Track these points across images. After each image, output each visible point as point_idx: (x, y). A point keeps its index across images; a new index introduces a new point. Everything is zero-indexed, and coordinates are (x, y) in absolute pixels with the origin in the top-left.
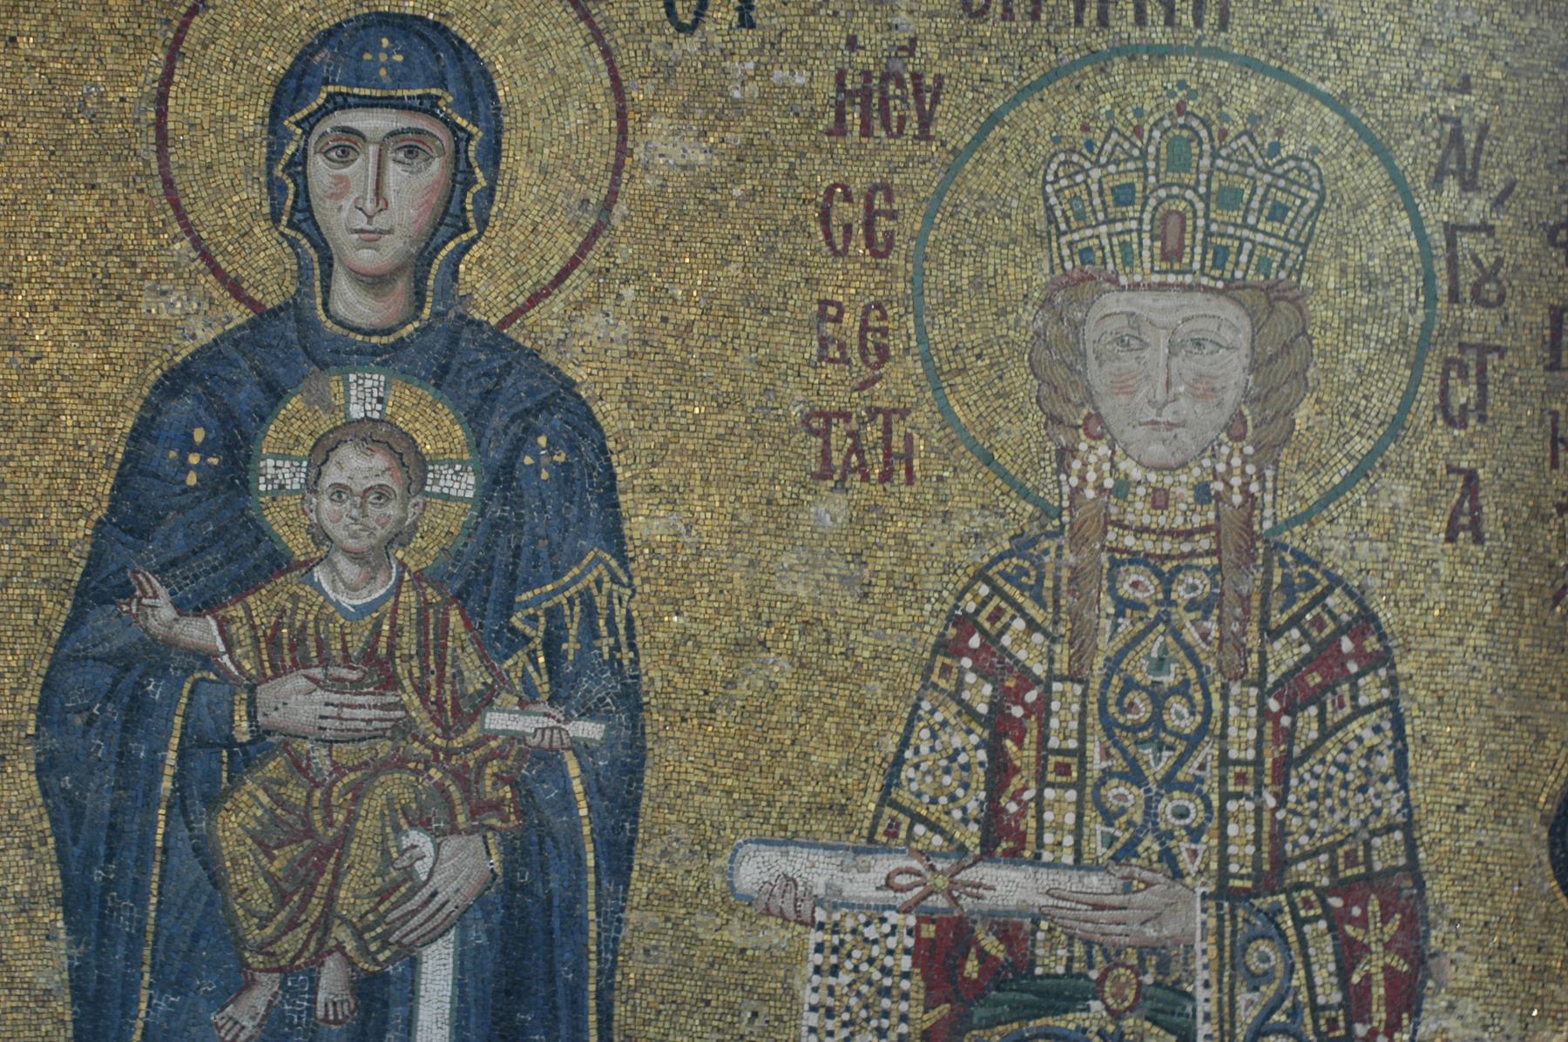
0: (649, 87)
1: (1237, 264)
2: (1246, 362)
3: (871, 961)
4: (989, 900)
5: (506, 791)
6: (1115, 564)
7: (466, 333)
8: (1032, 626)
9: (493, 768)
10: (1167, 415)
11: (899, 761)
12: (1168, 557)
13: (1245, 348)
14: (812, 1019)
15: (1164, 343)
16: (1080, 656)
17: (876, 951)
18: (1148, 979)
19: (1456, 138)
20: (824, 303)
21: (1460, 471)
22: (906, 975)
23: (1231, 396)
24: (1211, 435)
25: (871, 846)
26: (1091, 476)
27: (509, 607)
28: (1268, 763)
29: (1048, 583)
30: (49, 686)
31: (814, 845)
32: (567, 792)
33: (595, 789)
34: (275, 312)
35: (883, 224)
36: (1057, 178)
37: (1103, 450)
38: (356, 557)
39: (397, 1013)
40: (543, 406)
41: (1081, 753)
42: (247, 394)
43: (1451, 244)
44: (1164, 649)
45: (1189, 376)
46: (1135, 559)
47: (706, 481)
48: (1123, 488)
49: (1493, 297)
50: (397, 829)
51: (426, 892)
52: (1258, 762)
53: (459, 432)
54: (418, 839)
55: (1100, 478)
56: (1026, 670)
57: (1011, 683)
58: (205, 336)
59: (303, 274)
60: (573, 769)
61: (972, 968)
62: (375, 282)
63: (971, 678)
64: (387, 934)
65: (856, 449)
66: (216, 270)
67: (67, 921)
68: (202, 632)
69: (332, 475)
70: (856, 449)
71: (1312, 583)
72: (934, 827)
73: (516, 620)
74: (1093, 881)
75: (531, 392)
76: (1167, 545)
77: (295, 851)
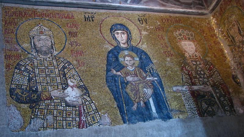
0: (141, 28)
3: (187, 95)
4: (195, 89)
5: (151, 84)
6: (192, 62)
7: (133, 47)
8: (188, 67)
9: (149, 82)
10: (190, 50)
11: (183, 78)
14: (185, 101)
17: (187, 94)
18: (210, 94)
19: (201, 30)
20: (161, 44)
22: (191, 96)
23: (194, 49)
24: (194, 51)
25: (183, 86)
27: (145, 69)
28: (210, 76)
30: (106, 79)
31: (179, 86)
32: (156, 84)
33: (159, 83)
34: (116, 46)
35: (163, 38)
38: (130, 66)
39: (149, 105)
40: (142, 52)
41: (196, 76)
42: (116, 53)
47: (158, 57)
48: (190, 56)
50: (143, 89)
51: (147, 94)
52: (209, 76)
53: (136, 55)
54: (145, 89)
58: (111, 49)
59: (117, 43)
60: (156, 82)
61: (196, 95)
62: (124, 44)
63: (185, 71)
64: (145, 98)
65: (168, 54)
66: (110, 43)
67: (115, 100)
68: (119, 73)
69: (126, 59)
70: (168, 54)
72: (188, 83)
73: (146, 70)
74: (202, 86)
75: (141, 51)
77: (135, 91)
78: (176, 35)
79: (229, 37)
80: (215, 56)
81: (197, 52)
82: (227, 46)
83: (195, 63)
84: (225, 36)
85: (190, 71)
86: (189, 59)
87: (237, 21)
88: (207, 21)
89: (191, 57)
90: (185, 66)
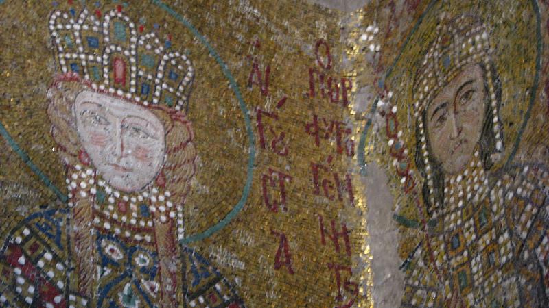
1: (155, 96)
2: (163, 147)
6: (99, 237)
8: (56, 259)
10: (123, 163)
12: (127, 239)
13: (162, 138)
15: (118, 125)
16: (82, 282)
19: (255, 66)
21: (278, 234)
23: (156, 163)
24: (147, 180)
26: (83, 185)
29: (64, 237)
36: (55, 25)
37: (89, 172)
43: (259, 118)
44: (130, 289)
45: (133, 146)
46: (109, 235)
48: (101, 198)
49: (283, 151)
55: (89, 187)
56: (52, 283)
57: (45, 289)
63: (21, 281)
71: (207, 275)
76: (128, 234)
78: (65, 34)
79: (420, 165)
80: (282, 260)
81: (162, 188)
82: (390, 222)
83: (118, 256)
84: (400, 158)
85: (60, 292)
86: (86, 214)
87: (493, 70)
88: (321, 24)
89: (104, 204)
90: (34, 248)
